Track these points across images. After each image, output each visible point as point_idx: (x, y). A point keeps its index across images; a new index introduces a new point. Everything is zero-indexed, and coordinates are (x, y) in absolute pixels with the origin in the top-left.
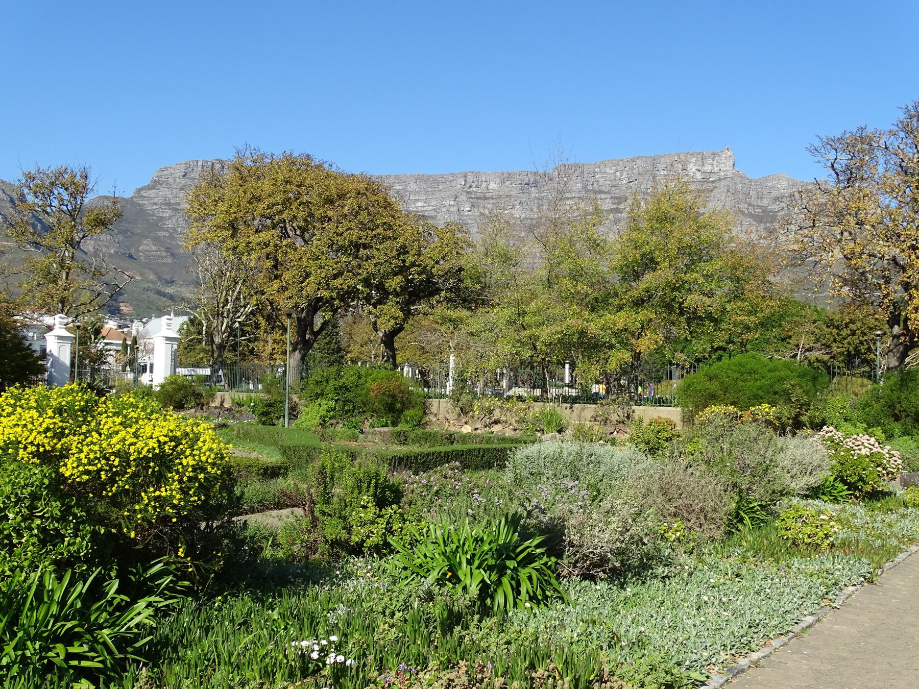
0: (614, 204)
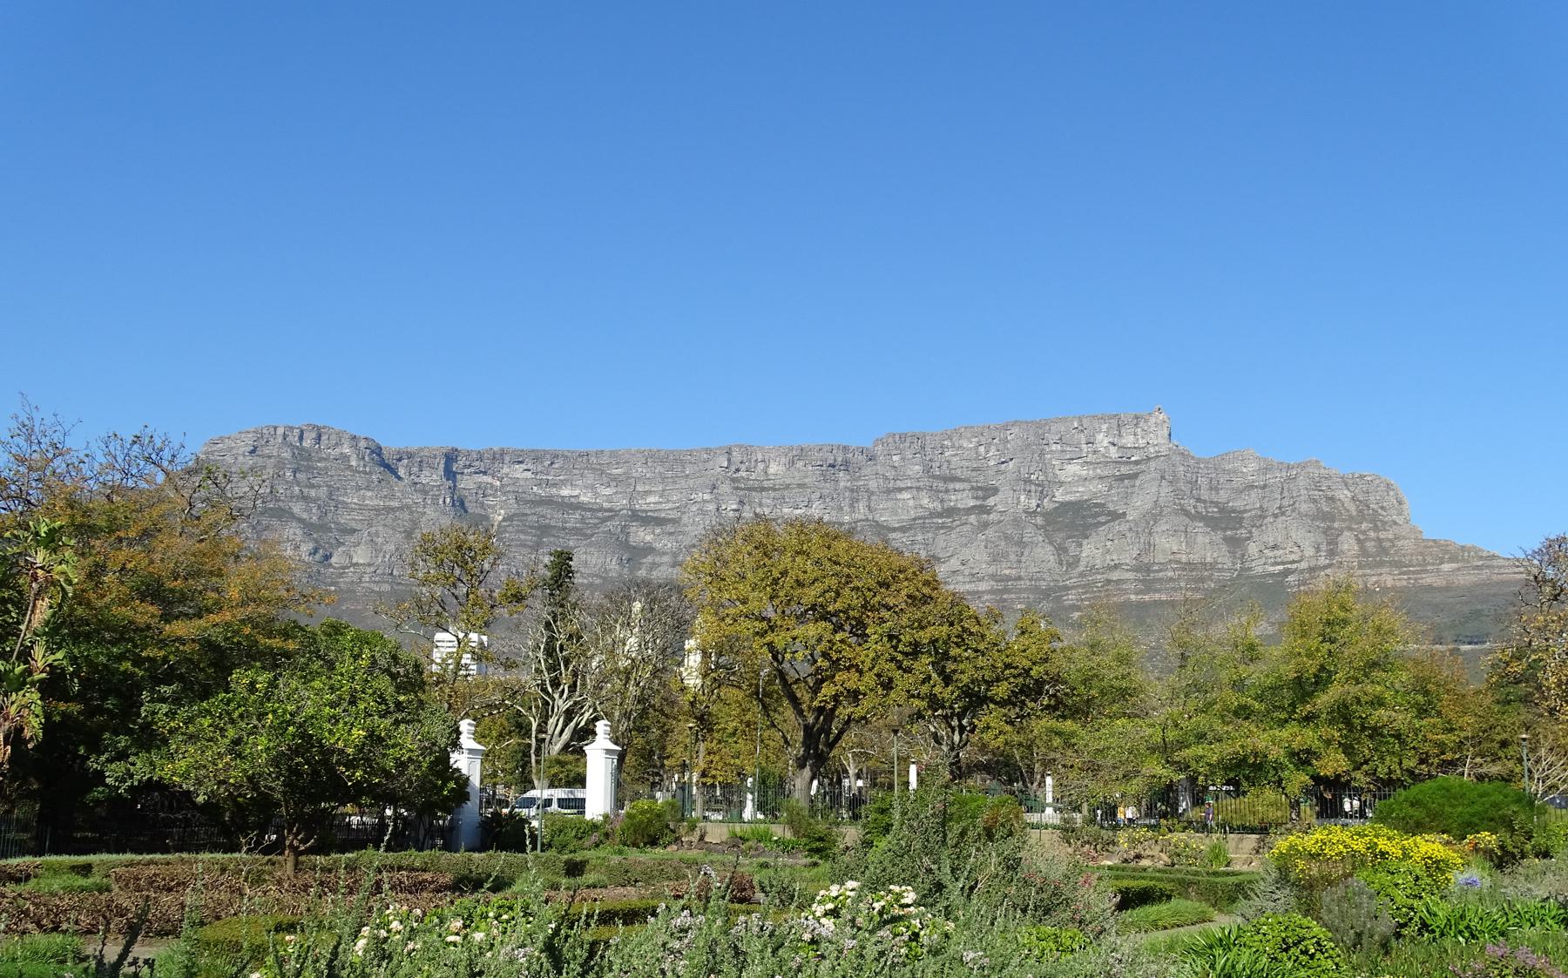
0: (977, 498)
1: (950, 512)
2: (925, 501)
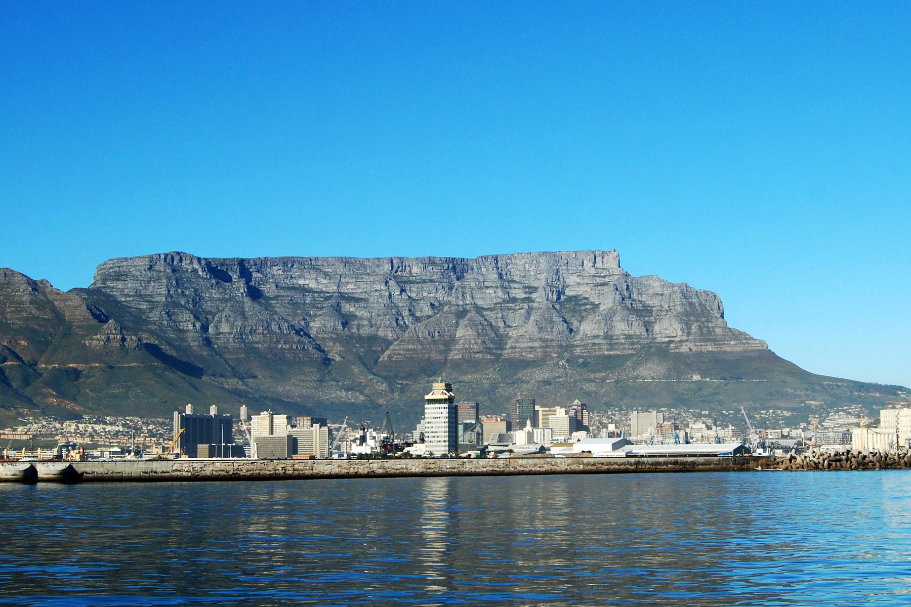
0: (526, 293)
1: (514, 300)
2: (500, 294)
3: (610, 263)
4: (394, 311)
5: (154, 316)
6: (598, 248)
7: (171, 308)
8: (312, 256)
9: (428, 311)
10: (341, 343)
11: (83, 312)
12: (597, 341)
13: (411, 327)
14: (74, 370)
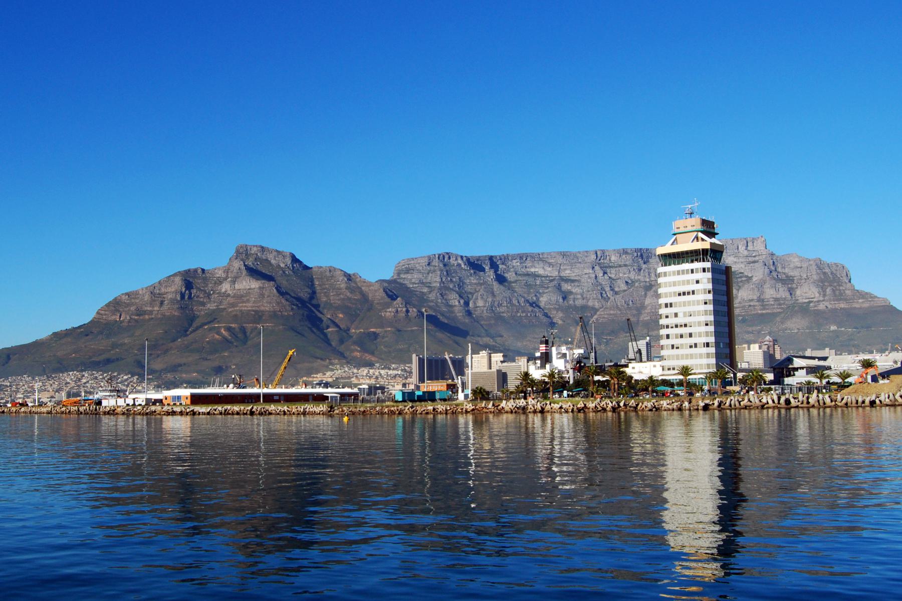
3: (759, 246)
4: (599, 288)
5: (432, 296)
6: (750, 236)
7: (443, 290)
8: (540, 251)
9: (623, 287)
10: (562, 311)
11: (381, 294)
12: (752, 304)
13: (612, 298)
14: (374, 333)
